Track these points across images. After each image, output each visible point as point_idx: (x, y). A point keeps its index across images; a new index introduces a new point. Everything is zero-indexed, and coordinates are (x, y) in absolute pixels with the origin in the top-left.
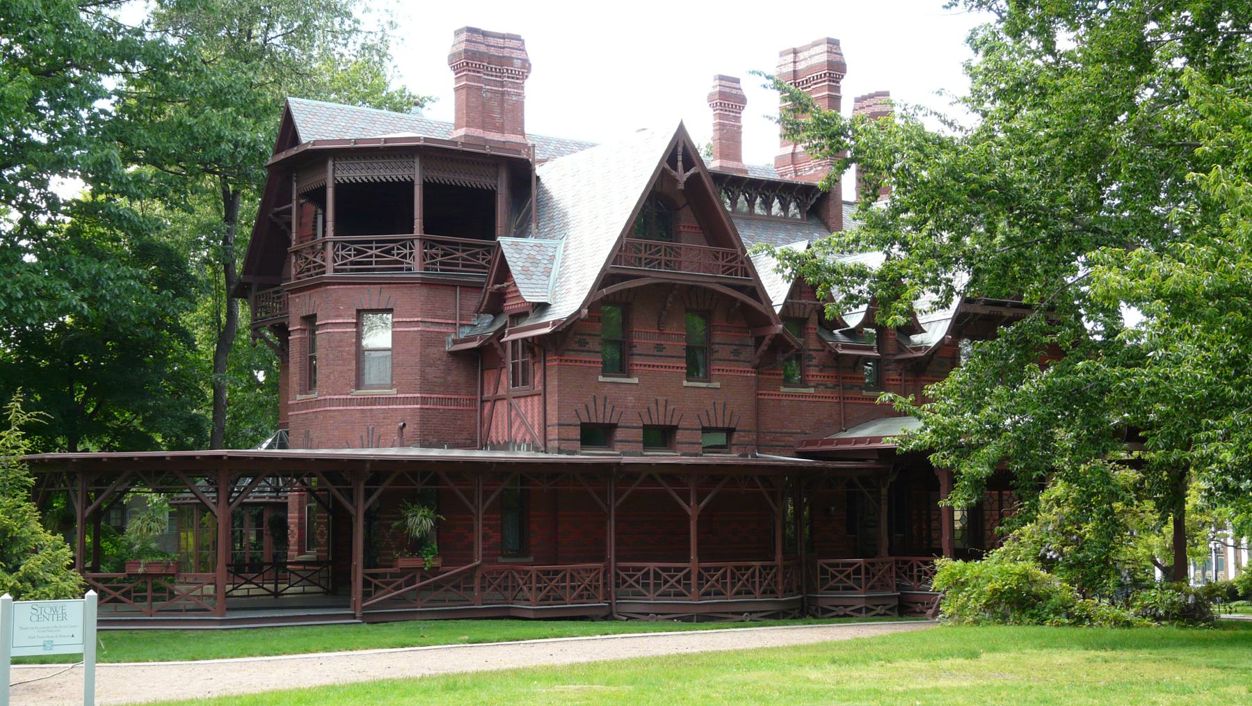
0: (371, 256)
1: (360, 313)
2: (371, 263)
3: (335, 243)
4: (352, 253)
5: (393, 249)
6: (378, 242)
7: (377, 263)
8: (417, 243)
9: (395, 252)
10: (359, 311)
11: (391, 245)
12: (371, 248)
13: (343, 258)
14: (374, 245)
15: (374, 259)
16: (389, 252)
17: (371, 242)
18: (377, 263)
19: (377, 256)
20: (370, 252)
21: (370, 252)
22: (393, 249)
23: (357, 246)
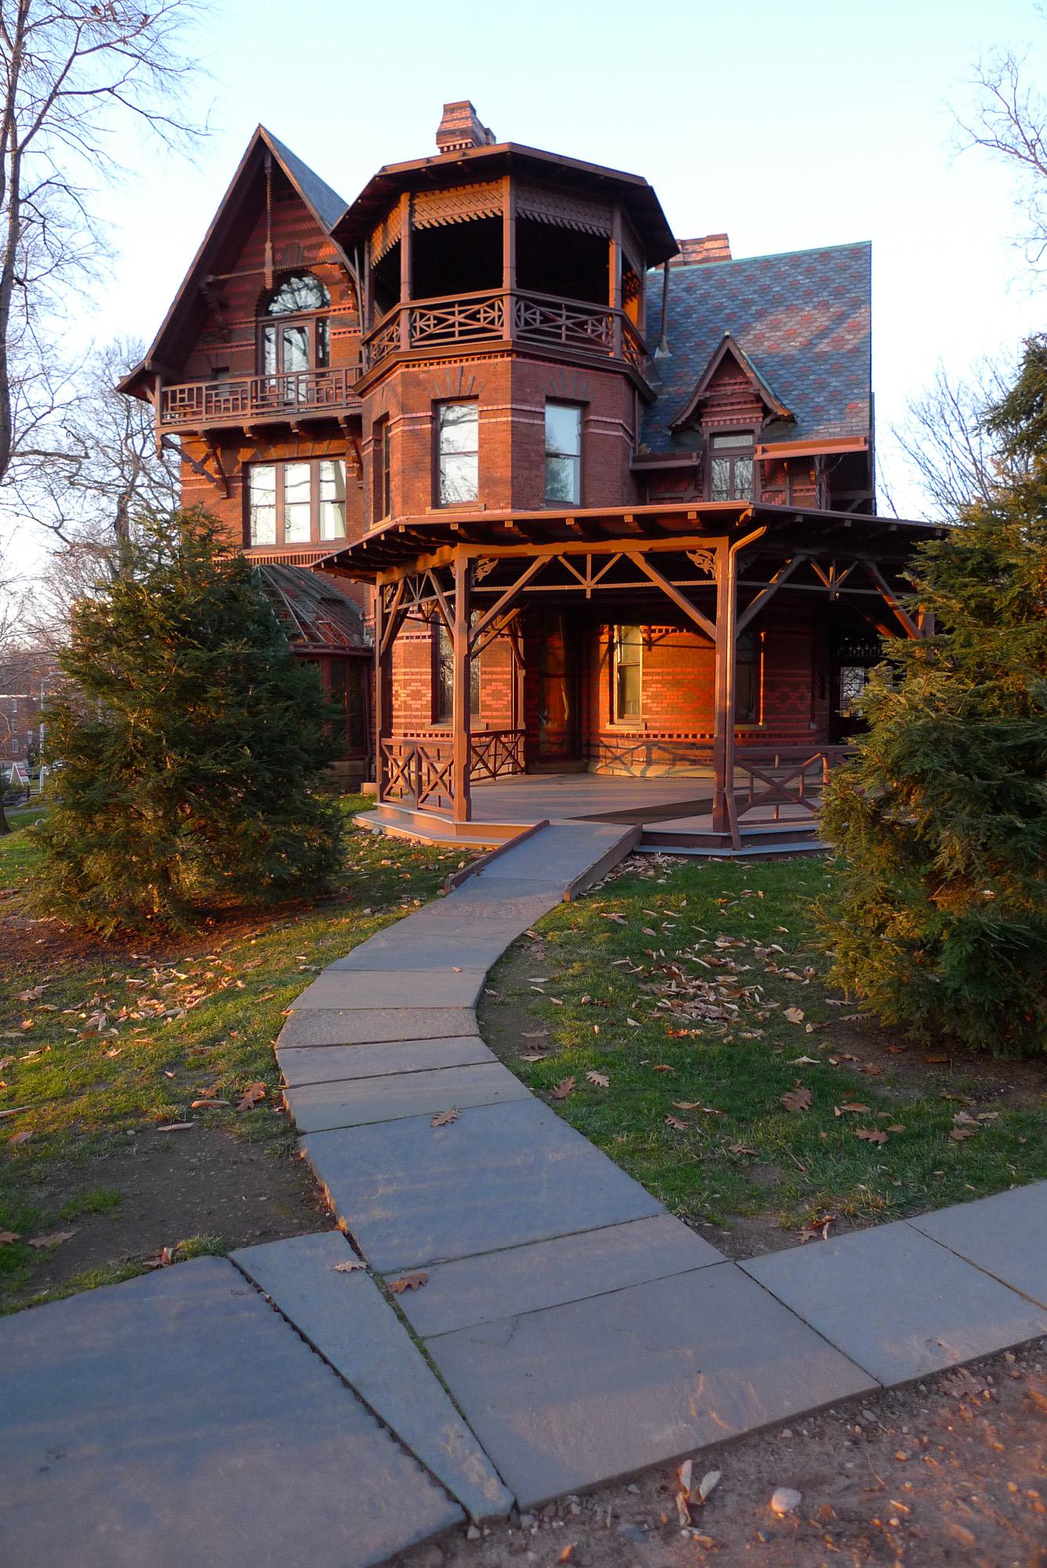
0: (453, 326)
1: (436, 403)
2: (452, 334)
3: (412, 310)
4: (432, 322)
5: (478, 312)
6: (461, 303)
7: (461, 333)
8: (506, 299)
9: (482, 316)
10: (436, 403)
11: (477, 307)
12: (453, 314)
13: (422, 331)
14: (456, 309)
15: (457, 329)
16: (473, 317)
17: (452, 305)
18: (461, 333)
19: (461, 324)
20: (452, 319)
21: (452, 319)
22: (478, 312)
23: (436, 313)
